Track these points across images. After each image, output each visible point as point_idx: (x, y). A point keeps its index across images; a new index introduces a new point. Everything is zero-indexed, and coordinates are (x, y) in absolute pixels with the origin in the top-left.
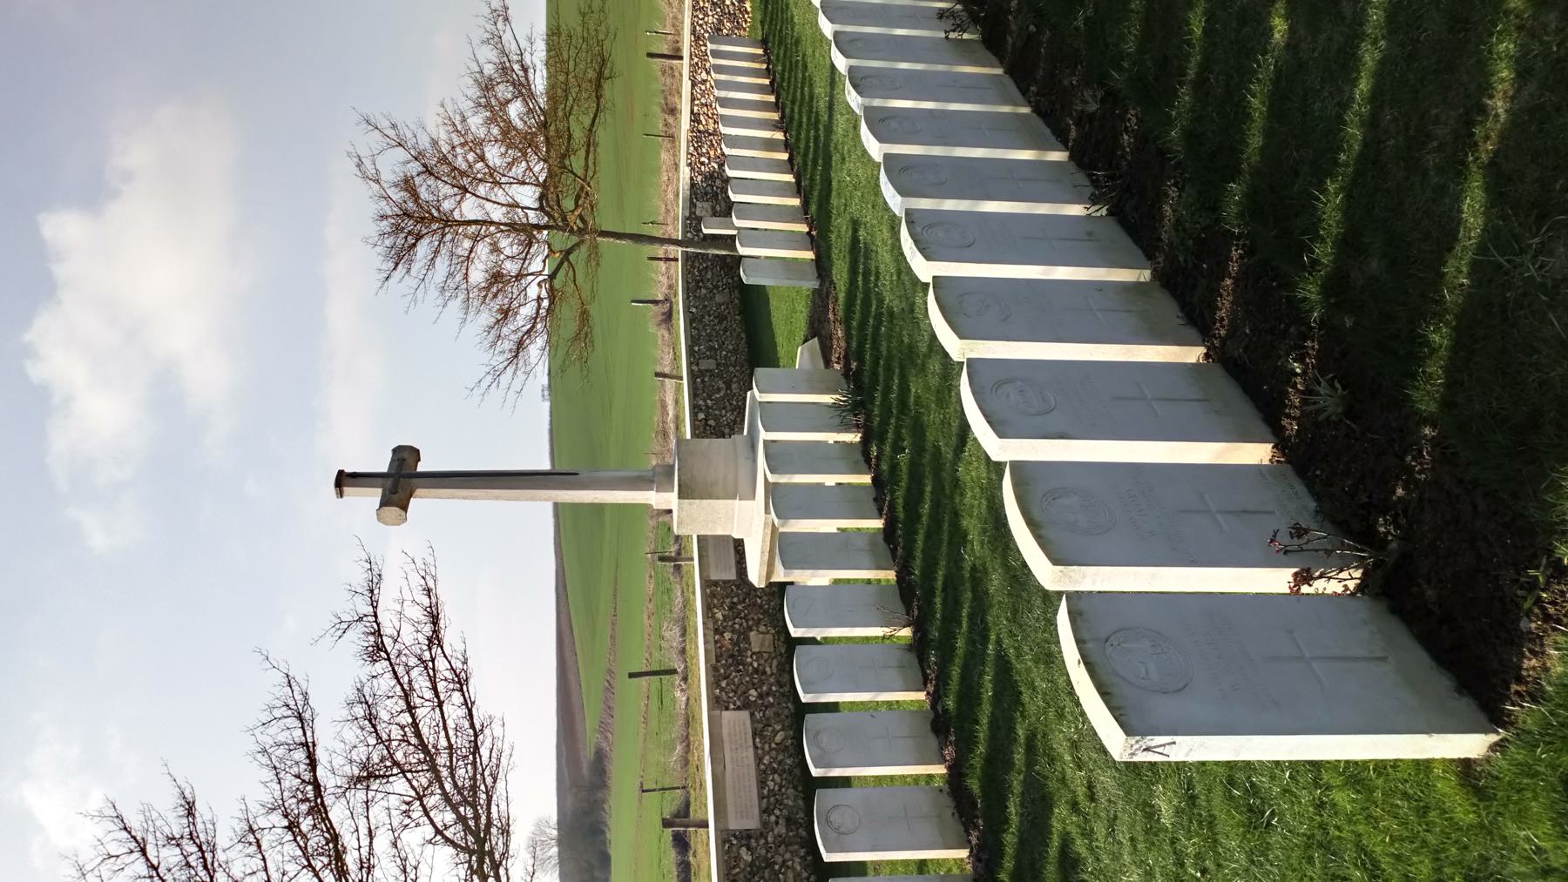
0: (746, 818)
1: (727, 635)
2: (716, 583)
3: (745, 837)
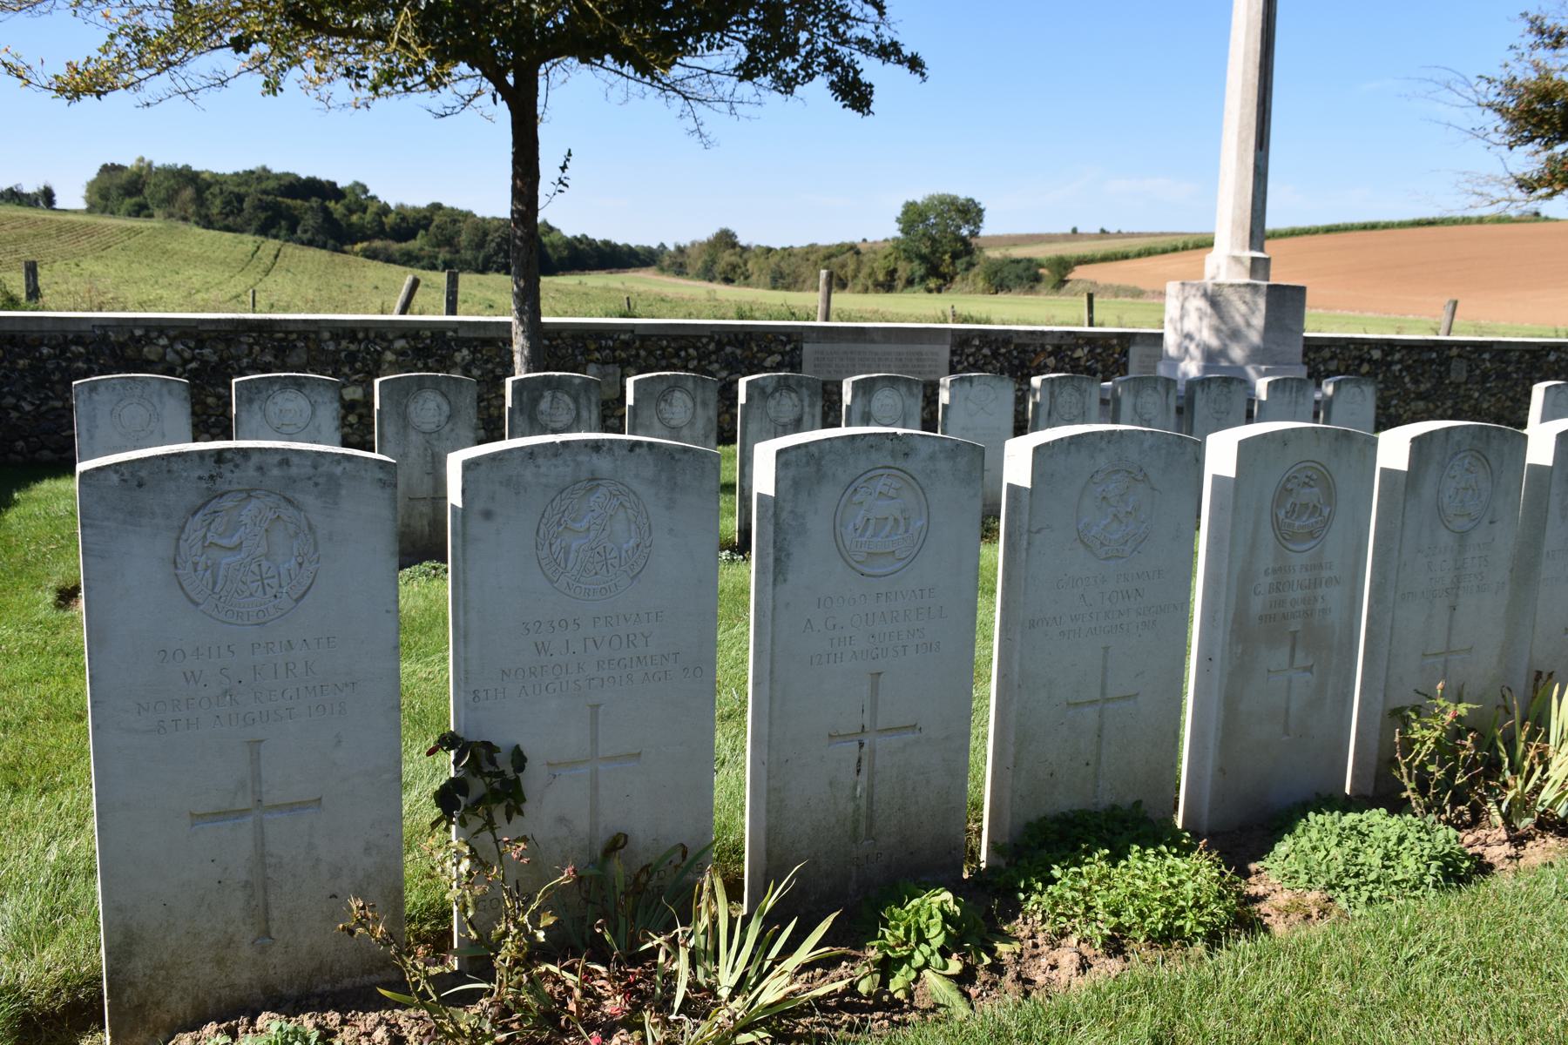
2: (1125, 353)
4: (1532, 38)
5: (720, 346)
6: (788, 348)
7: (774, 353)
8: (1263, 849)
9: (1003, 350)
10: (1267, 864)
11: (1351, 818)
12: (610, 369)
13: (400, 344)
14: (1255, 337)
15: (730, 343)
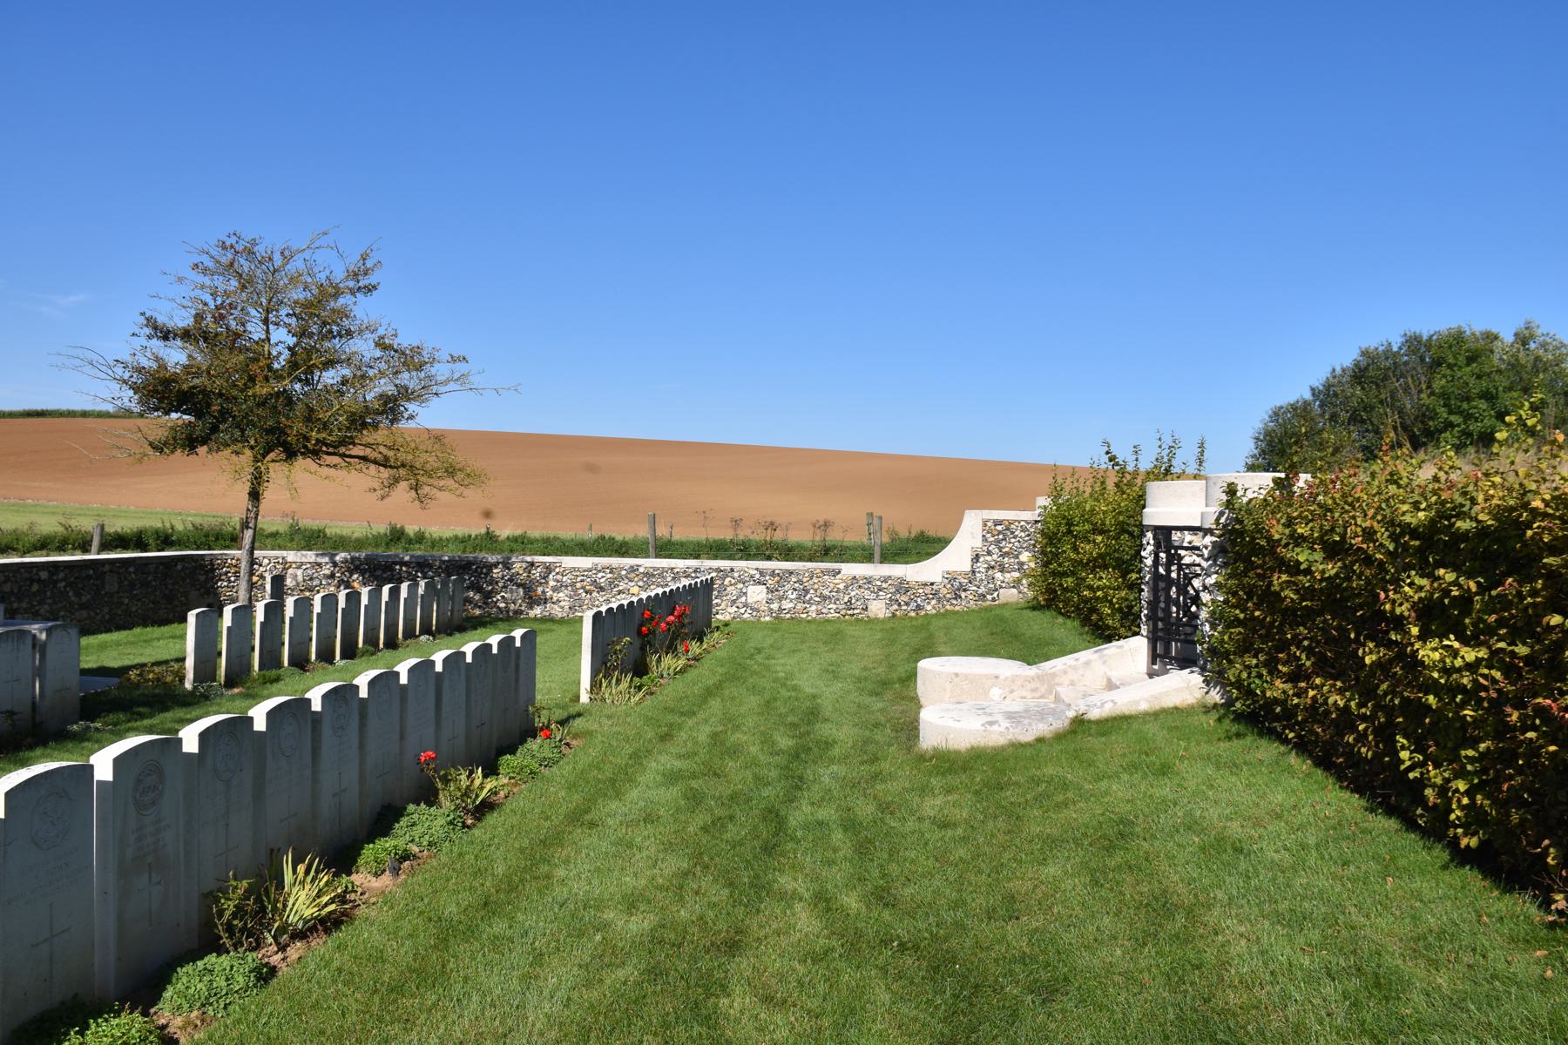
4: (148, 331)
8: (155, 998)
10: (160, 1005)
11: (200, 964)
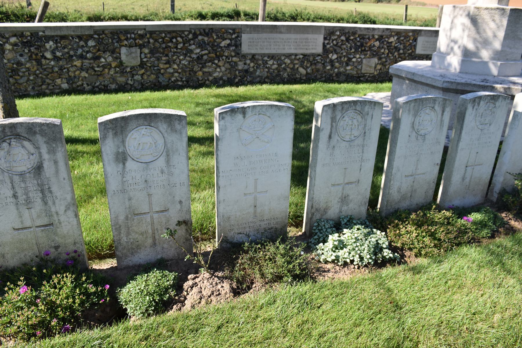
0: (249, 45)
1: (377, 44)
2: (415, 40)
3: (238, 45)
5: (195, 36)
6: (234, 36)
7: (226, 39)
9: (352, 38)
12: (133, 49)
13: (13, 40)
14: (497, 45)
15: (201, 34)
